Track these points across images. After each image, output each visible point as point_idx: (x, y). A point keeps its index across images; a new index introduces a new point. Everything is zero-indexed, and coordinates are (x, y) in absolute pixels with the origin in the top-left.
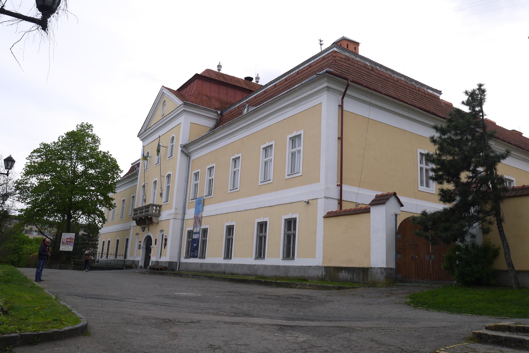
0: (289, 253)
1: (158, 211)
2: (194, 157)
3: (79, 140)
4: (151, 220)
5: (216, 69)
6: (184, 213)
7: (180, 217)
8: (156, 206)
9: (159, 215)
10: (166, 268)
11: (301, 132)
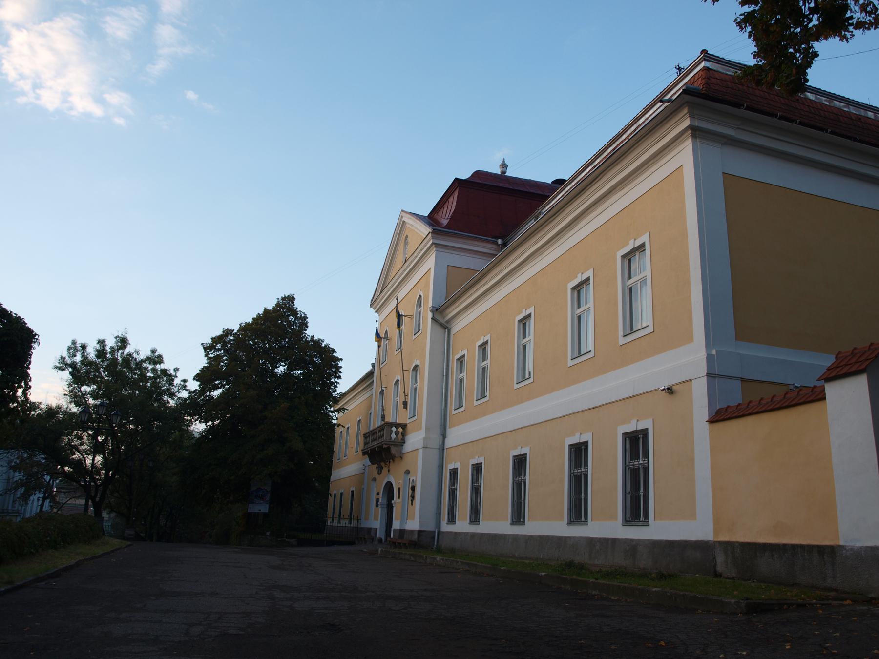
0: (636, 509)
1: (400, 436)
2: (458, 326)
3: (280, 325)
4: (388, 449)
5: (498, 171)
6: (444, 436)
7: (435, 443)
8: (398, 425)
9: (403, 442)
10: (414, 545)
11: (645, 238)
